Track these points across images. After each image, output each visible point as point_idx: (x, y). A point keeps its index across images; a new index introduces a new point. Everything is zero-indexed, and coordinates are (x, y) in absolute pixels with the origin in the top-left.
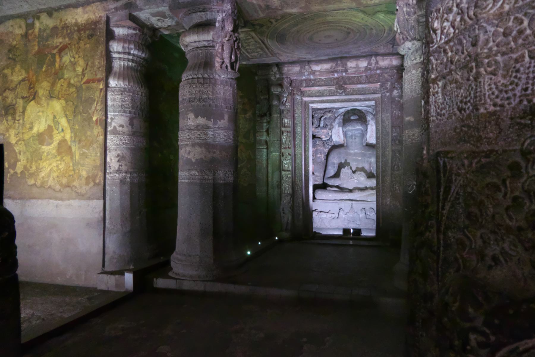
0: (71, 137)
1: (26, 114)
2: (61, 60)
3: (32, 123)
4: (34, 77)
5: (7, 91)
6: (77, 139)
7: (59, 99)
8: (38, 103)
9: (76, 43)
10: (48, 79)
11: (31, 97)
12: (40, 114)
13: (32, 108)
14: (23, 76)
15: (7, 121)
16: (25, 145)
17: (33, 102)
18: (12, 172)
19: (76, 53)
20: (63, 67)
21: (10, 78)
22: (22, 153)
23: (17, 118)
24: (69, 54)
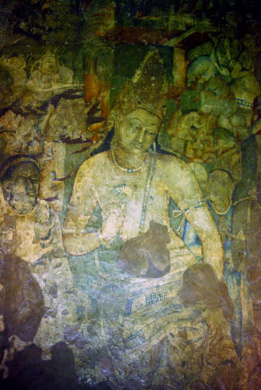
0: (225, 262)
1: (76, 185)
2: (189, 67)
3: (98, 212)
4: (106, 96)
5: (11, 114)
6: (242, 267)
7: (185, 159)
8: (118, 161)
9: (232, 35)
10: (149, 106)
11: (96, 145)
12: (127, 190)
13: (97, 174)
14: (69, 85)
15: (9, 196)
16: (74, 269)
17: (101, 157)
18: (19, 344)
19: (236, 59)
20: (195, 83)
21: (20, 81)
22: (59, 293)
23: (46, 192)
24: (212, 56)
